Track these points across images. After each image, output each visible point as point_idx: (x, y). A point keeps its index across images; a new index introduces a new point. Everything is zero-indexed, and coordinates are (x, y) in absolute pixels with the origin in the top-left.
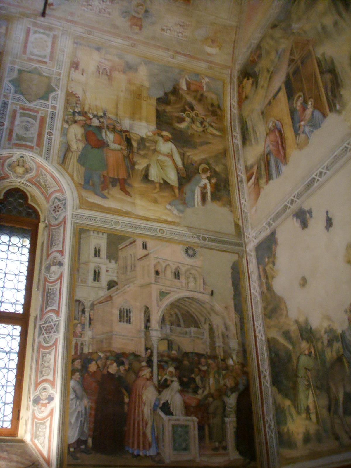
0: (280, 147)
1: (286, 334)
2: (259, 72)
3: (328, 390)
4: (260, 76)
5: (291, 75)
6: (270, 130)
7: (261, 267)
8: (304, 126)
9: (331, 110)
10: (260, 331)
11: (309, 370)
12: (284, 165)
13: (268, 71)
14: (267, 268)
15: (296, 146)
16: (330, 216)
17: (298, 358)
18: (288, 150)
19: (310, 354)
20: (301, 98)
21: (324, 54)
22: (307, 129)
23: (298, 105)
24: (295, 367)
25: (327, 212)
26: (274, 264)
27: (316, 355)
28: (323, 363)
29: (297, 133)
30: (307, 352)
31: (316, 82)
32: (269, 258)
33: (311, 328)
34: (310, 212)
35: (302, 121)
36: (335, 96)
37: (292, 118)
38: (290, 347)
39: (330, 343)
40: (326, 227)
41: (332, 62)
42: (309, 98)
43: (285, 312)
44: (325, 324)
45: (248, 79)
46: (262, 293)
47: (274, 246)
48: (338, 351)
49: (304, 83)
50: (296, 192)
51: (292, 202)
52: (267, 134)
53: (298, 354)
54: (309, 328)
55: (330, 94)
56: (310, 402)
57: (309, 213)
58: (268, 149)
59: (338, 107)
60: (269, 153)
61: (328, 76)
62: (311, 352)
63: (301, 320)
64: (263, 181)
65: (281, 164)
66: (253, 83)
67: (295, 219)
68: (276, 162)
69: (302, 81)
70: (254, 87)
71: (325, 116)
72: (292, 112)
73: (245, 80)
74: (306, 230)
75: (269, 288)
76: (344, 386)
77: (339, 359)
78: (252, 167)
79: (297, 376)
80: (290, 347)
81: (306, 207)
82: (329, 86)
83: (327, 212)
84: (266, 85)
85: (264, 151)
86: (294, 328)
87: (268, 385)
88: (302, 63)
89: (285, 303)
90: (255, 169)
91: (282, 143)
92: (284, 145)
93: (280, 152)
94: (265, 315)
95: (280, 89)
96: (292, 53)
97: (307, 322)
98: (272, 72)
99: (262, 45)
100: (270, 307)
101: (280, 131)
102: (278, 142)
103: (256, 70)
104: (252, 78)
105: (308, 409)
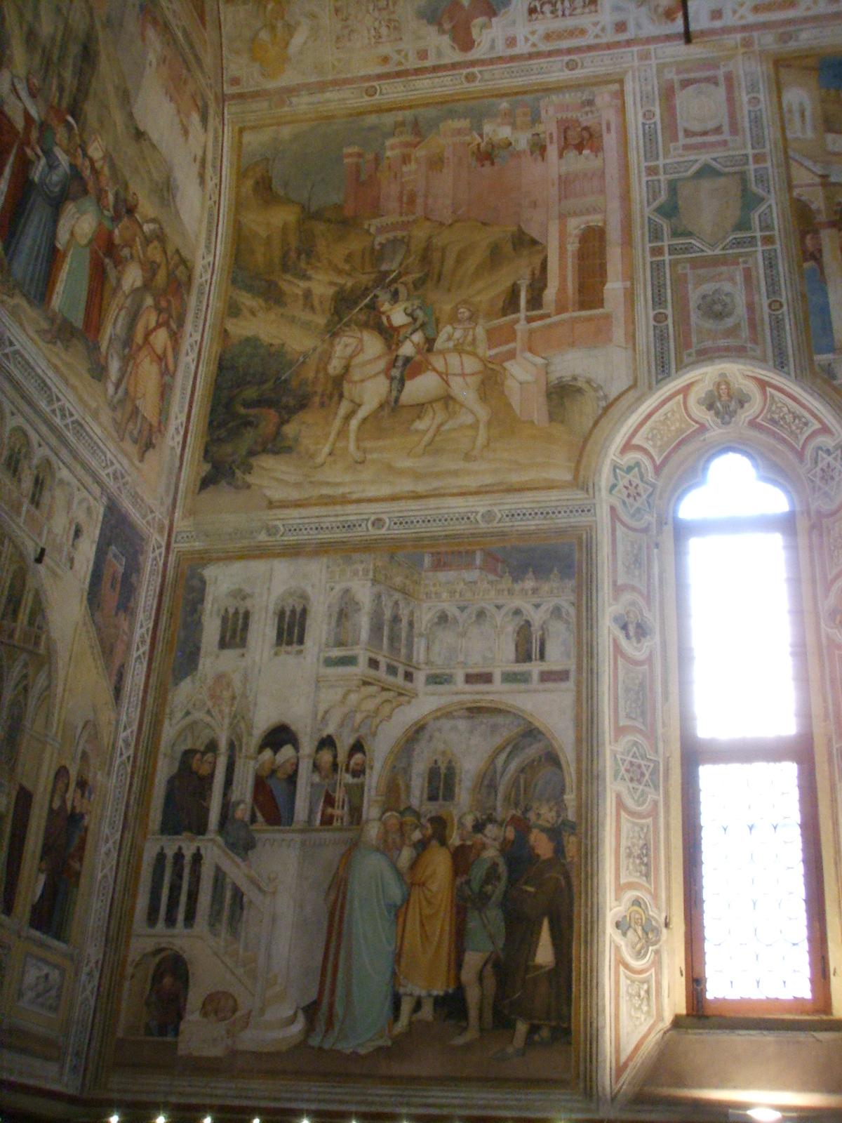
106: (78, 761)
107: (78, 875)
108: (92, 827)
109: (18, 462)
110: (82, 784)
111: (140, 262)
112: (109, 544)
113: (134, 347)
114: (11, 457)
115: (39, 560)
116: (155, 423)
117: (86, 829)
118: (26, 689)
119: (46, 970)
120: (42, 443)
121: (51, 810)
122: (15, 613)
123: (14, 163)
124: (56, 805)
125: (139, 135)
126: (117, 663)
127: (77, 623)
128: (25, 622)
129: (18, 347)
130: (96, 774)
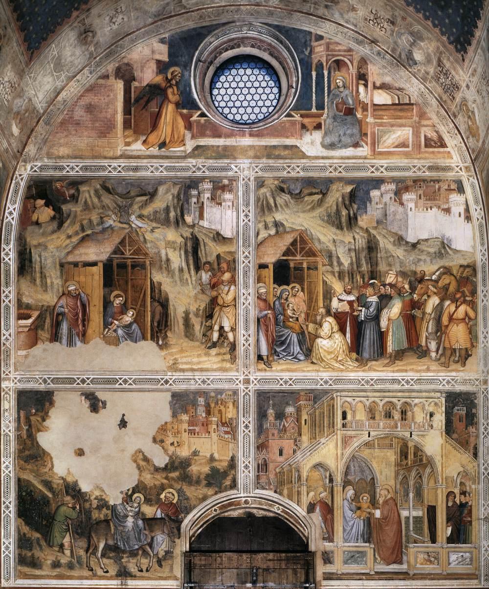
0: (80, 322)
1: (48, 484)
2: (69, 216)
3: (89, 538)
4: (68, 221)
5: (115, 264)
6: (69, 292)
7: (22, 413)
8: (118, 327)
9: (152, 339)
10: (7, 467)
11: (70, 519)
12: (82, 342)
13: (83, 229)
14: (32, 418)
15: (102, 336)
16: (126, 419)
17: (58, 508)
18: (90, 331)
19: (74, 508)
20: (121, 299)
21: (160, 284)
22: (120, 332)
23: (118, 302)
24: (53, 512)
25: (124, 415)
26: (44, 420)
27: (80, 510)
28: (89, 518)
29: (106, 325)
30: (70, 505)
31: (144, 300)
32: (37, 411)
33: (80, 490)
34: (104, 404)
35: (117, 320)
36: (161, 331)
37: (105, 308)
38: (50, 495)
39: (99, 508)
40: (119, 425)
41: (167, 300)
42: (132, 308)
43: (50, 465)
44: (97, 493)
45: (47, 205)
46: (19, 438)
47: (47, 404)
48: (106, 515)
49: (130, 287)
50: (92, 377)
51: (83, 381)
52: (63, 294)
53: (60, 504)
54: (78, 489)
55: (156, 324)
56: (67, 541)
57: (102, 403)
58: (62, 309)
59: (160, 342)
60: (63, 314)
61: (159, 309)
62: (76, 507)
63: (70, 479)
64: (44, 334)
65: (77, 339)
66: (53, 218)
67: (83, 398)
68: (70, 330)
69: (127, 282)
70: (55, 224)
71: (144, 338)
72: (107, 303)
73: (41, 202)
74: (93, 414)
75: (31, 436)
76: (106, 540)
77: (107, 521)
78: (28, 307)
79: (53, 519)
80: (50, 495)
81: (101, 395)
82: (157, 317)
83: (124, 415)
84: (75, 240)
85: (55, 306)
86: (57, 482)
87: (12, 515)
88: (133, 267)
89: (51, 458)
90: (35, 314)
91: (84, 320)
92: (86, 323)
93: (78, 326)
94: (18, 456)
95: (94, 264)
96: (122, 242)
97: (76, 483)
98: (87, 235)
99: (83, 188)
100: (27, 453)
101: (84, 306)
102: (77, 314)
103: (65, 208)
104: (54, 210)
105: (62, 546)
106: (459, 486)
107: (470, 522)
108: (474, 504)
109: (390, 413)
110: (463, 493)
111: (435, 293)
112: (454, 407)
113: (443, 328)
114: (386, 414)
115: (411, 436)
116: (468, 345)
117: (471, 506)
118: (420, 477)
119: (461, 554)
120: (399, 399)
121: (448, 507)
122: (406, 458)
123: (350, 323)
124: (450, 504)
125: (414, 246)
126: (472, 445)
127: (442, 444)
128: (412, 457)
129: (376, 378)
130: (470, 487)
